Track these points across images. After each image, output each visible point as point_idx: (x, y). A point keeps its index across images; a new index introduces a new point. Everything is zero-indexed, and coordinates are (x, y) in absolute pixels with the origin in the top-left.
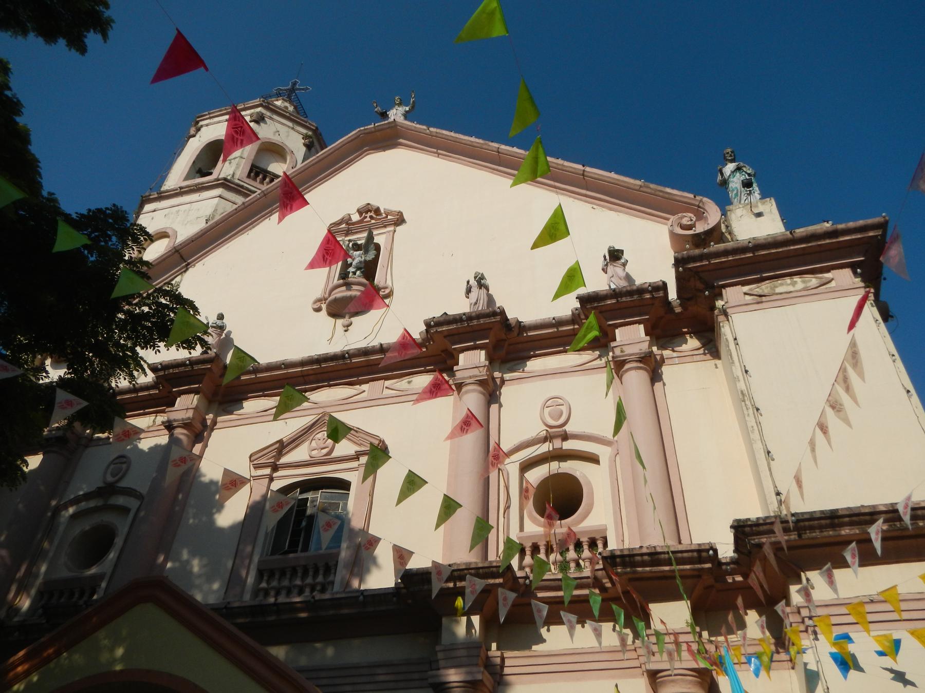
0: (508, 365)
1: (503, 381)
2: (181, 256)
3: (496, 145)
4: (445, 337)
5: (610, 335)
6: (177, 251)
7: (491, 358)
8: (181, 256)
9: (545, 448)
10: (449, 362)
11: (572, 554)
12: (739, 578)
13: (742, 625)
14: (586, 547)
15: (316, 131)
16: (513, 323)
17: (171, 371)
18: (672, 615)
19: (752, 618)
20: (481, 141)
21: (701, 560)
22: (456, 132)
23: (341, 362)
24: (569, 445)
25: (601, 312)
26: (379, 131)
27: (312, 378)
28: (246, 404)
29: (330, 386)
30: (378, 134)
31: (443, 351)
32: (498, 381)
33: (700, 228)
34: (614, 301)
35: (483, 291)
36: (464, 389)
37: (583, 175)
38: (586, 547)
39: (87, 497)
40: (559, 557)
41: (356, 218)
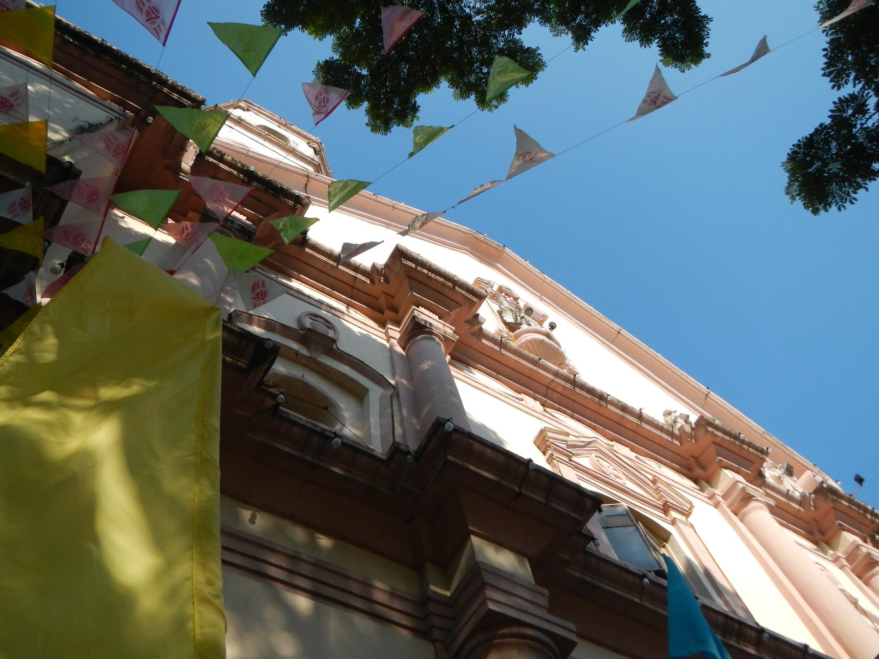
2: (306, 185)
4: (714, 443)
5: (828, 535)
6: (308, 177)
8: (306, 185)
10: (698, 471)
17: (425, 271)
23: (597, 400)
25: (834, 508)
26: (486, 244)
27: (555, 395)
28: (474, 371)
29: (573, 417)
30: (484, 245)
31: (693, 457)
34: (847, 504)
36: (753, 504)
37: (707, 395)
39: (285, 330)
41: (495, 288)
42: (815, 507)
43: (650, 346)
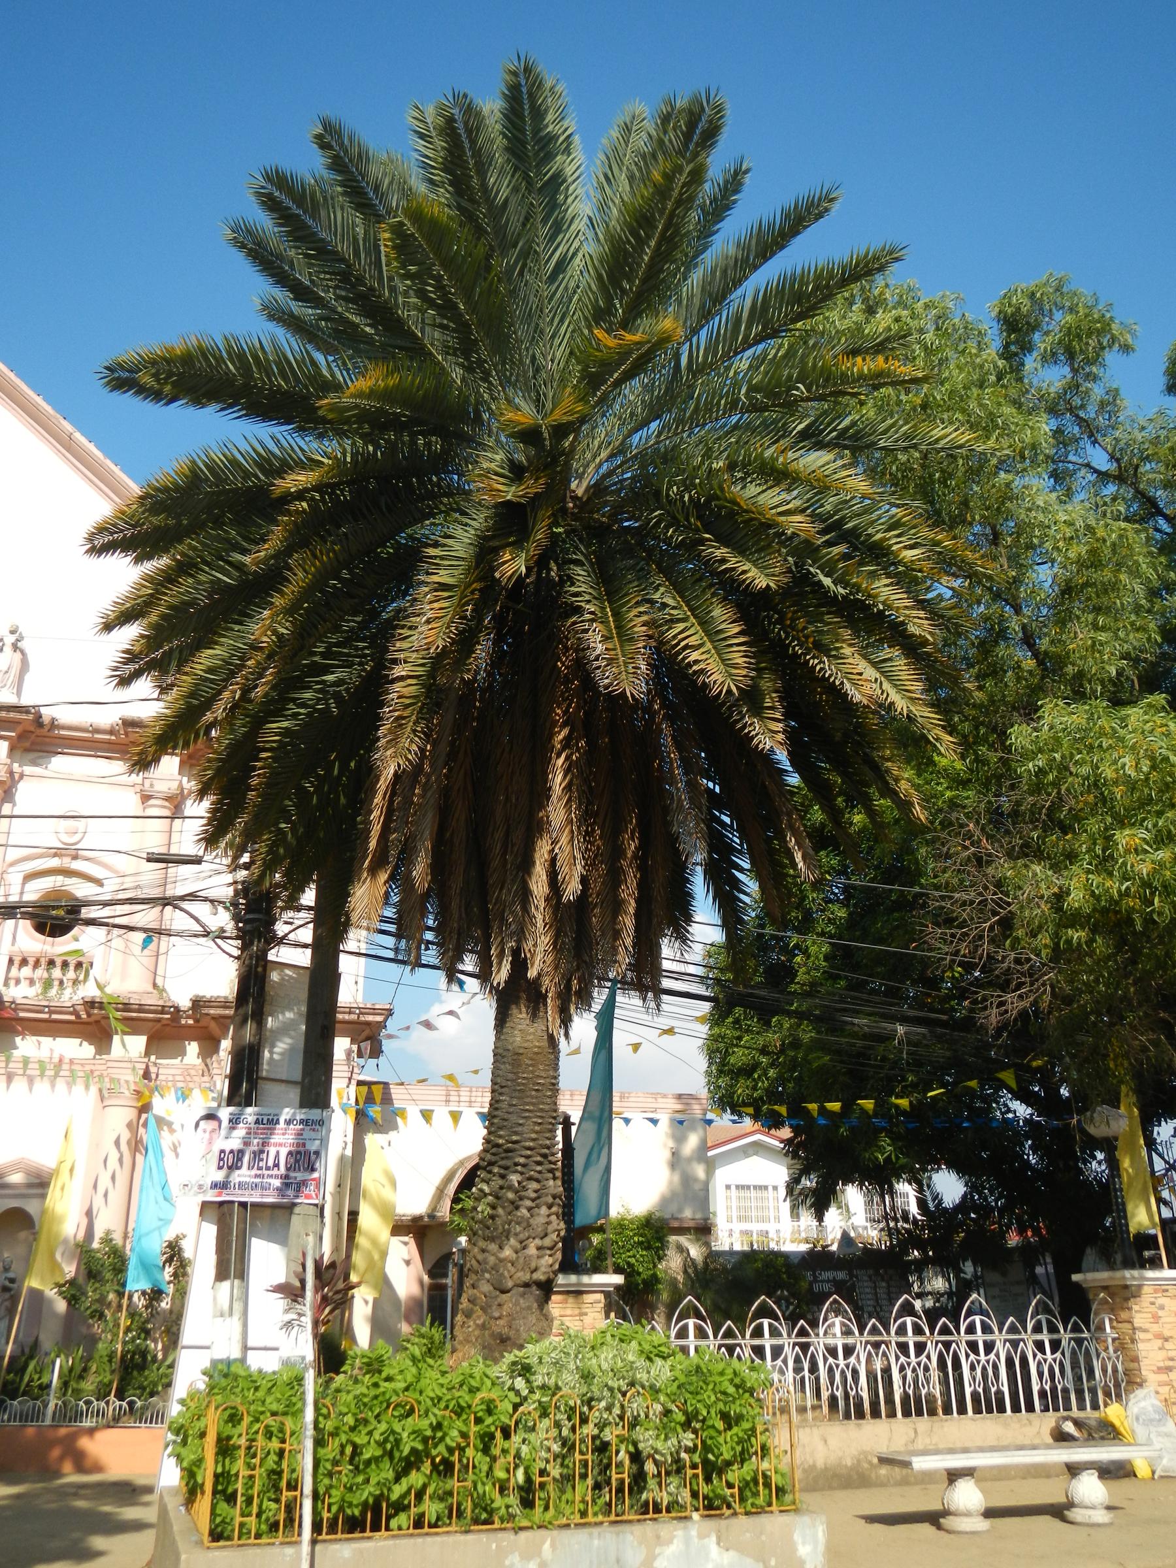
0: (32, 755)
1: (22, 776)
3: (67, 426)
7: (12, 749)
9: (55, 863)
11: (57, 973)
12: (191, 1022)
13: (183, 1053)
14: (72, 968)
16: (46, 720)
18: (131, 1047)
19: (193, 1048)
20: (49, 409)
21: (162, 1012)
22: (17, 375)
24: (77, 865)
32: (17, 776)
35: (18, 655)
38: (72, 968)
40: (46, 975)
42: (126, 734)
43: (107, 455)
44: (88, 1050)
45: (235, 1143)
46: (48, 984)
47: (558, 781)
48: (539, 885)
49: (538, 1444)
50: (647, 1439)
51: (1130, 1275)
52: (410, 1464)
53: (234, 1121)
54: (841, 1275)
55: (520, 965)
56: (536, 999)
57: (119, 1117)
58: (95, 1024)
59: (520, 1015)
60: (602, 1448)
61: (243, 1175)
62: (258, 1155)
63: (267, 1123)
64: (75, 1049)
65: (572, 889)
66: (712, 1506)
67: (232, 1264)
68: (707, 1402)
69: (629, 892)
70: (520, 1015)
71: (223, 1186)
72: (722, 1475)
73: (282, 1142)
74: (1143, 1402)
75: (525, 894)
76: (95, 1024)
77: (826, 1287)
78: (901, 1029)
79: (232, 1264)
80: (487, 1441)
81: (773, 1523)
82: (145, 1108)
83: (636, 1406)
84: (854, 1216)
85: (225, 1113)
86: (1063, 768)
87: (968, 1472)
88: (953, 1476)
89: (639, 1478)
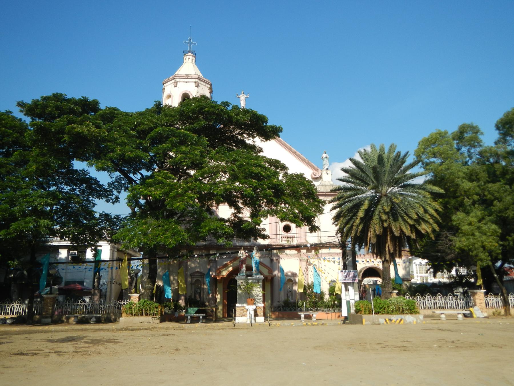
15: (211, 85)
19: (313, 251)
33: (317, 176)
44: (296, 252)
45: (345, 275)
46: (288, 241)
47: (389, 238)
48: (387, 249)
49: (393, 307)
50: (404, 307)
51: (475, 291)
52: (381, 308)
53: (345, 272)
54: (438, 289)
55: (385, 258)
56: (387, 261)
57: (304, 264)
58: (298, 248)
59: (385, 263)
60: (399, 308)
61: (347, 278)
62: (349, 276)
63: (349, 272)
64: (293, 252)
65: (392, 251)
66: (411, 313)
67: (347, 290)
68: (410, 304)
69: (397, 249)
70: (385, 263)
71: (345, 280)
72: (412, 310)
73: (352, 274)
74: (476, 308)
75: (385, 250)
76: (298, 248)
77: (436, 291)
78: (439, 254)
79: (347, 290)
80: (388, 307)
81: (417, 315)
82: (307, 261)
83: (402, 304)
84: (443, 278)
85: (344, 271)
86: (459, 224)
87: (443, 313)
88: (442, 314)
89: (403, 311)
